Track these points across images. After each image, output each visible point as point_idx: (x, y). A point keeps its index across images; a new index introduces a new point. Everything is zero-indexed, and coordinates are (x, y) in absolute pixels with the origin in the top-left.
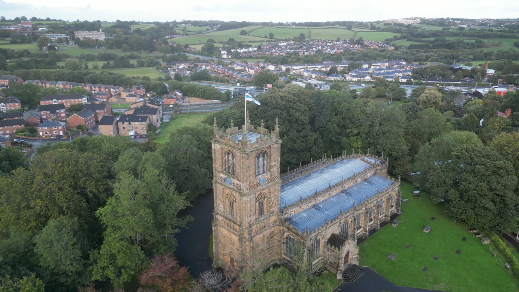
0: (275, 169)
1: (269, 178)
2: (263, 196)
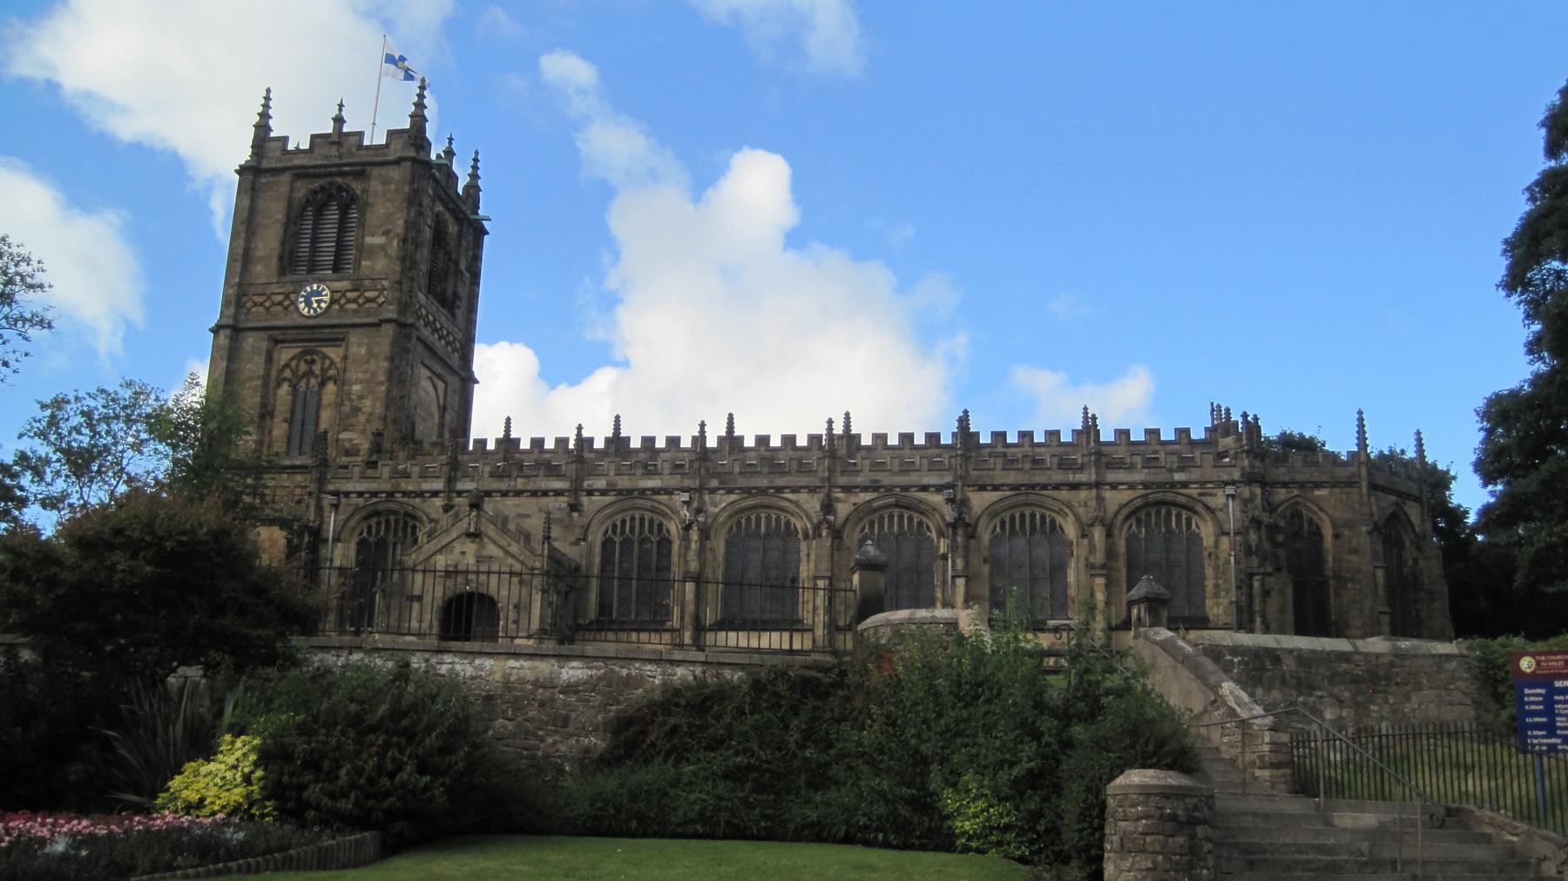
0: (381, 264)
1: (349, 295)
2: (317, 368)
